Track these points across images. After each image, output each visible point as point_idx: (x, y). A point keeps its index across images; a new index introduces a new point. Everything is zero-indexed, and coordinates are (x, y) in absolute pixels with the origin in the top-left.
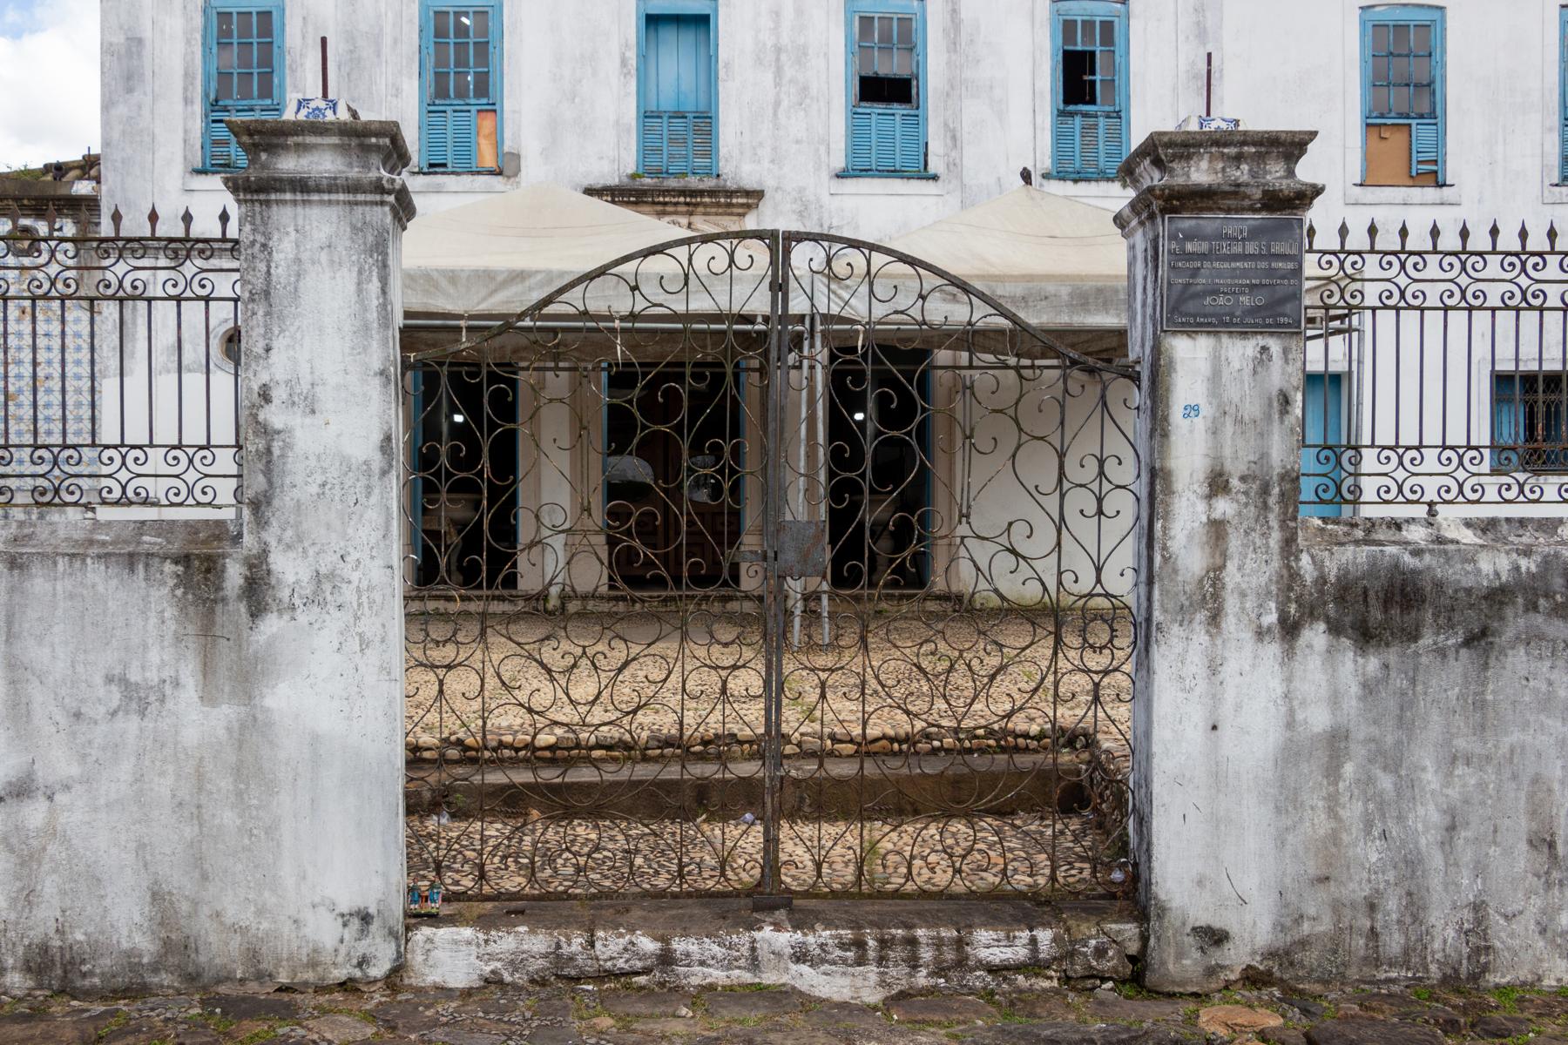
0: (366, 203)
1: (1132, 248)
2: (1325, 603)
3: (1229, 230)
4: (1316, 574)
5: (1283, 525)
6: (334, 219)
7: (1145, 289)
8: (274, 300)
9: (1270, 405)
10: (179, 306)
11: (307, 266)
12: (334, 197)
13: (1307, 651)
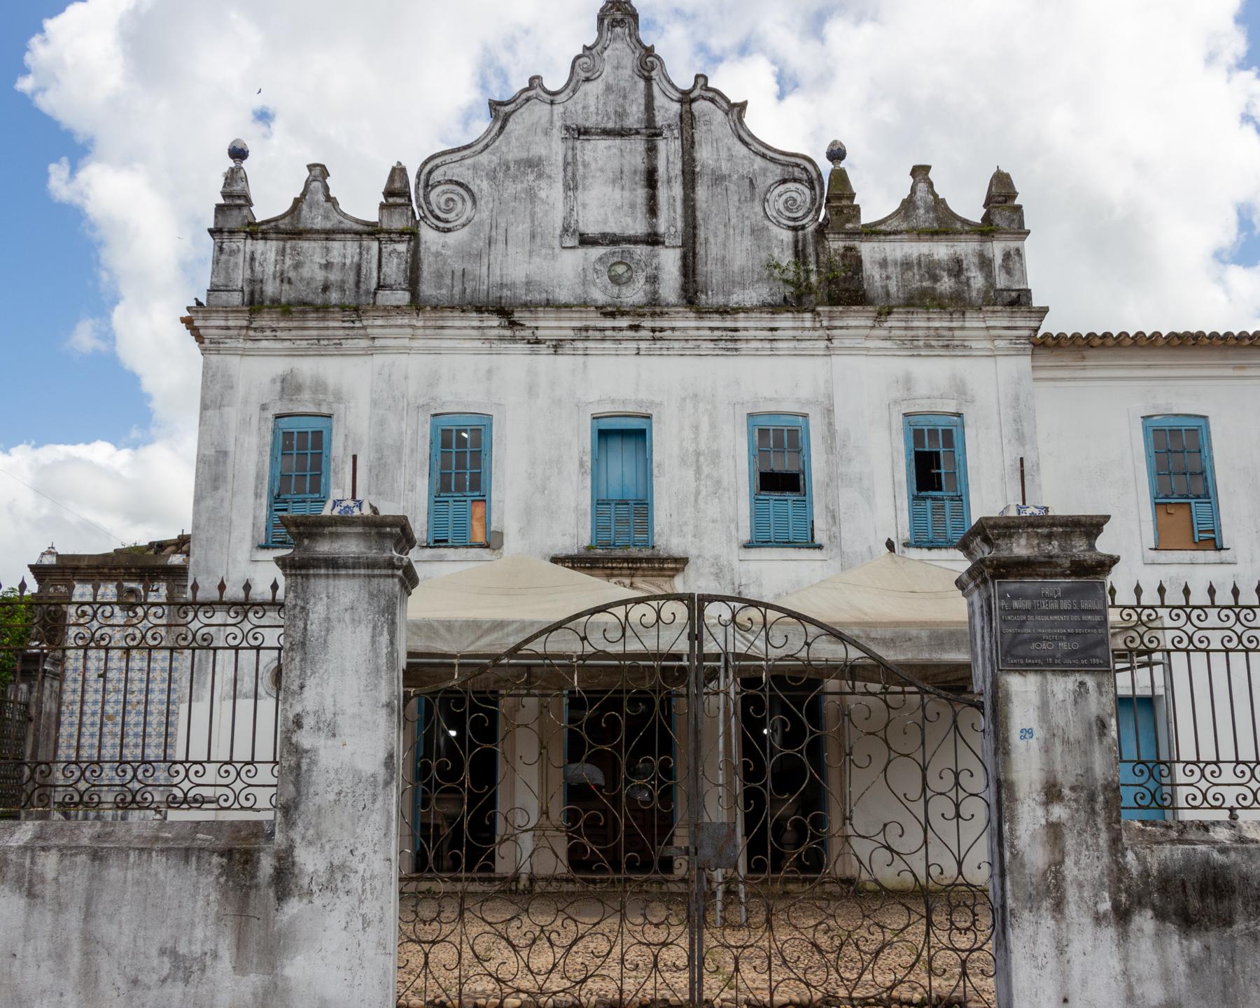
0: (381, 576)
1: (971, 605)
2: (1150, 893)
3: (1047, 591)
4: (1140, 868)
5: (1109, 827)
6: (357, 588)
7: (983, 636)
8: (309, 649)
9: (1090, 729)
10: (237, 654)
11: (335, 623)
12: (357, 572)
13: (1139, 934)
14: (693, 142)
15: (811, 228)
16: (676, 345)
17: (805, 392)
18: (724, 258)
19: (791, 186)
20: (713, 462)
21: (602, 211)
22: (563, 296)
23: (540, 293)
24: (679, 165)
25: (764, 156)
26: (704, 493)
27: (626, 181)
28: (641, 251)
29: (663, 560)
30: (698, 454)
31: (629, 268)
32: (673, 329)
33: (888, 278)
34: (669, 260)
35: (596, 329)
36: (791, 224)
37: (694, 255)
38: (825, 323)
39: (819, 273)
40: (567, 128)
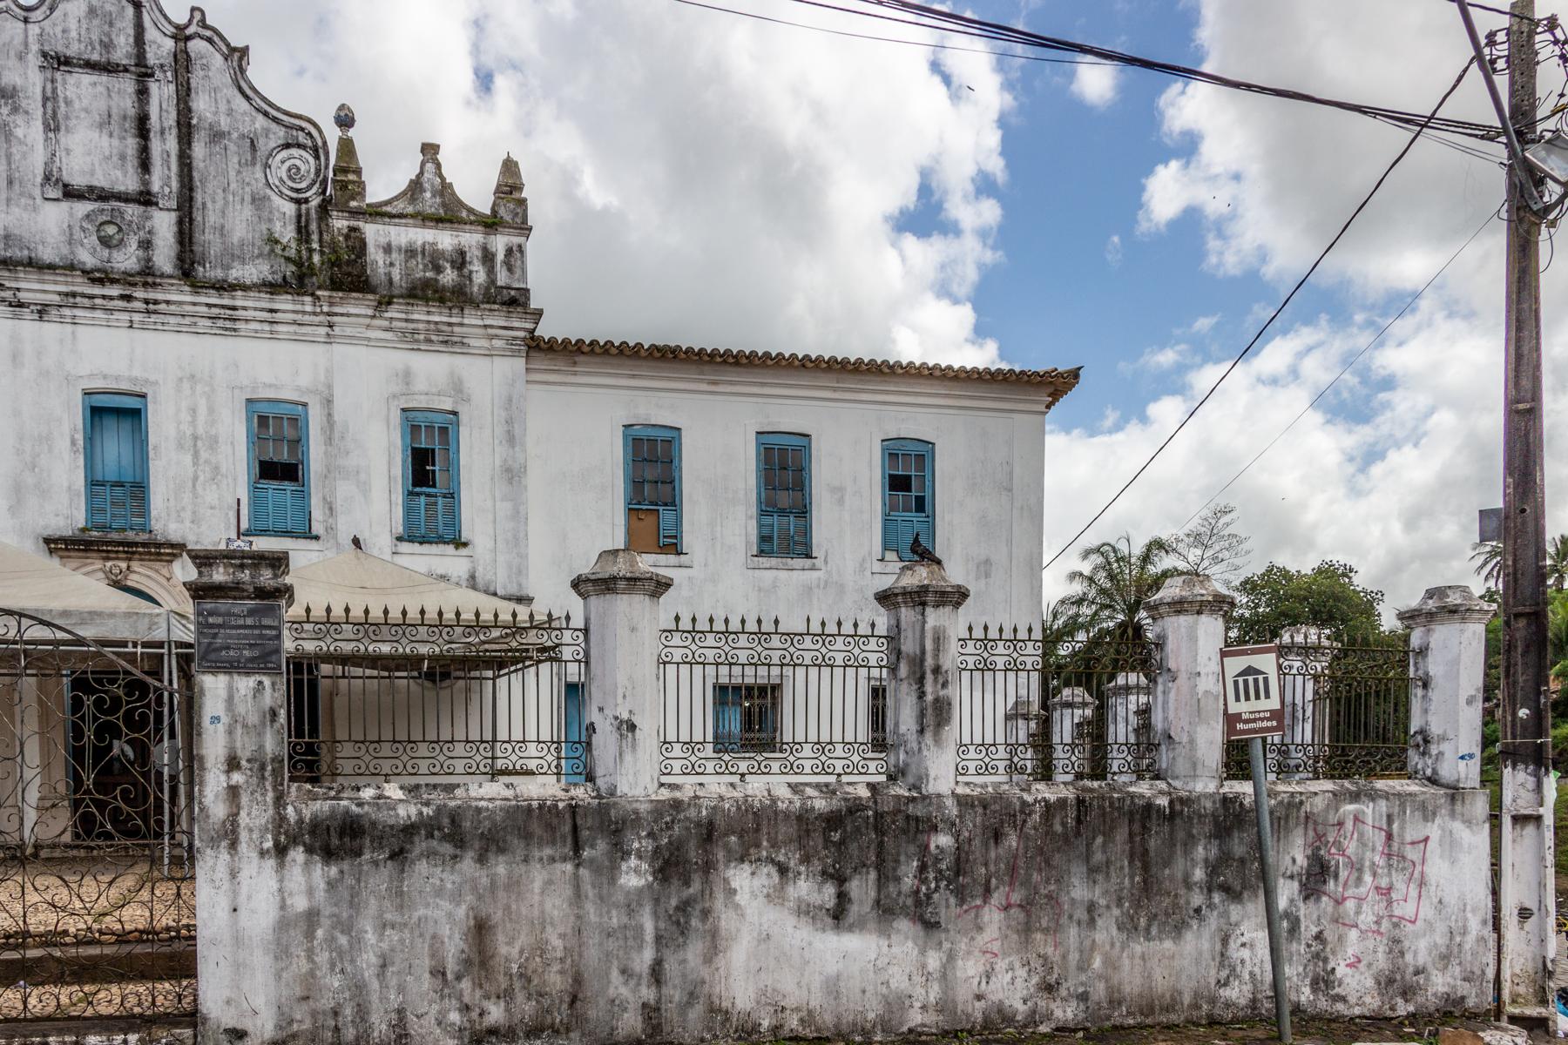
14: (189, 89)
15: (315, 203)
16: (172, 320)
17: (304, 380)
18: (223, 227)
19: (295, 152)
20: (211, 448)
21: (88, 159)
22: (47, 255)
23: (21, 249)
24: (174, 115)
25: (266, 114)
26: (202, 478)
27: (115, 127)
28: (132, 211)
29: (159, 545)
30: (195, 438)
31: (120, 229)
32: (168, 302)
33: (392, 264)
34: (164, 224)
35: (84, 296)
36: (294, 195)
37: (191, 221)
38: (325, 309)
39: (322, 253)
40: (45, 55)
